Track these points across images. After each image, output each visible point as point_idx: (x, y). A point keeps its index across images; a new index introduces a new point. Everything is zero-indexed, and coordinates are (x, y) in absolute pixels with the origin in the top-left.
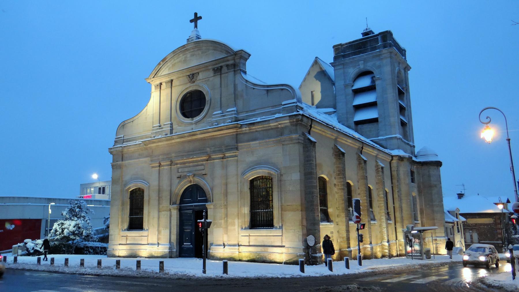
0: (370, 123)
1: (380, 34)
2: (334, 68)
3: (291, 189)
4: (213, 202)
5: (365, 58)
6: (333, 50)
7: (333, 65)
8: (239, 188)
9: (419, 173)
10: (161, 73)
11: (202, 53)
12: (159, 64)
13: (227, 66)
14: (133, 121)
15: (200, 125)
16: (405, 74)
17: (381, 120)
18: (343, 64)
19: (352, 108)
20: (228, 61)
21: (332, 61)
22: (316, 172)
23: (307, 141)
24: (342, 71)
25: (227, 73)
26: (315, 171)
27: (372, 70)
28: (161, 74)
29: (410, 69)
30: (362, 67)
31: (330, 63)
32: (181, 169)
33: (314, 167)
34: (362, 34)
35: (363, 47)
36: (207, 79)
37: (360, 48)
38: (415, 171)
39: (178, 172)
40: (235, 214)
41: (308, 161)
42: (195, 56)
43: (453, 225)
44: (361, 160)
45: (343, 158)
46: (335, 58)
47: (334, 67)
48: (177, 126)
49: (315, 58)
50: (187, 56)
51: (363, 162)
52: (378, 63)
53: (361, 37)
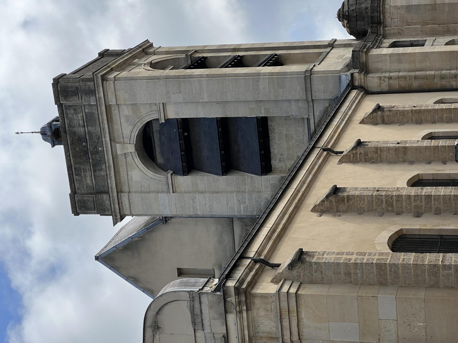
0: (268, 137)
1: (57, 101)
2: (128, 215)
3: (421, 324)
6: (82, 216)
7: (119, 217)
9: (400, 34)
16: (160, 53)
17: (263, 110)
19: (227, 176)
21: (110, 219)
22: (379, 255)
23: (295, 272)
24: (135, 198)
26: (377, 257)
27: (140, 125)
29: (149, 42)
30: (131, 148)
31: (115, 224)
33: (366, 257)
34: (53, 146)
35: (84, 144)
37: (86, 152)
38: (392, 41)
41: (348, 274)
44: (356, 153)
45: (348, 190)
46: (103, 211)
47: (125, 216)
49: (97, 261)
51: (360, 150)
52: (126, 111)
53: (60, 149)
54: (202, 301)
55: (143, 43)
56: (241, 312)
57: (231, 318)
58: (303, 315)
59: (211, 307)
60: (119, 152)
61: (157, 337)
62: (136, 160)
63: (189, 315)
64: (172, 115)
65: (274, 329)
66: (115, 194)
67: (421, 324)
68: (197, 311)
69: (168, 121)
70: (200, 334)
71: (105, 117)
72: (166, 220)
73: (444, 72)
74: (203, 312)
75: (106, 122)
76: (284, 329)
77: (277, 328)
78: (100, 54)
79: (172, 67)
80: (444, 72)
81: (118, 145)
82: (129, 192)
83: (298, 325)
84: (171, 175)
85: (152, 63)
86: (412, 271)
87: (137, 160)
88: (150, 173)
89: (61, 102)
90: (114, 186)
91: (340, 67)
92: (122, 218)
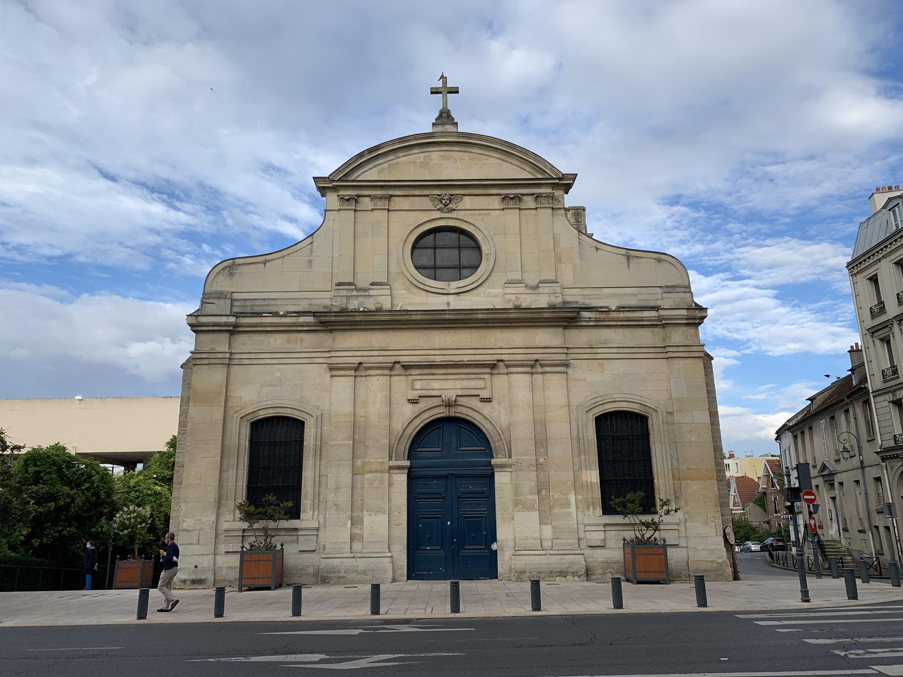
3: (693, 439)
4: (510, 457)
8: (575, 432)
10: (359, 176)
11: (471, 159)
12: (361, 155)
13: (538, 197)
14: (268, 264)
15: (468, 297)
20: (539, 185)
25: (536, 209)
28: (356, 178)
32: (419, 382)
36: (485, 212)
39: (413, 389)
40: (569, 483)
42: (452, 160)
48: (405, 292)
50: (430, 156)
54: (686, 293)
56: (687, 319)
57: (684, 312)
58: (687, 361)
59: (683, 299)
61: (653, 261)
63: (672, 284)
65: (674, 341)
67: (693, 439)
68: (678, 290)
70: (659, 290)
74: (678, 294)
76: (677, 348)
77: (675, 342)
83: (680, 357)
86: (716, 435)
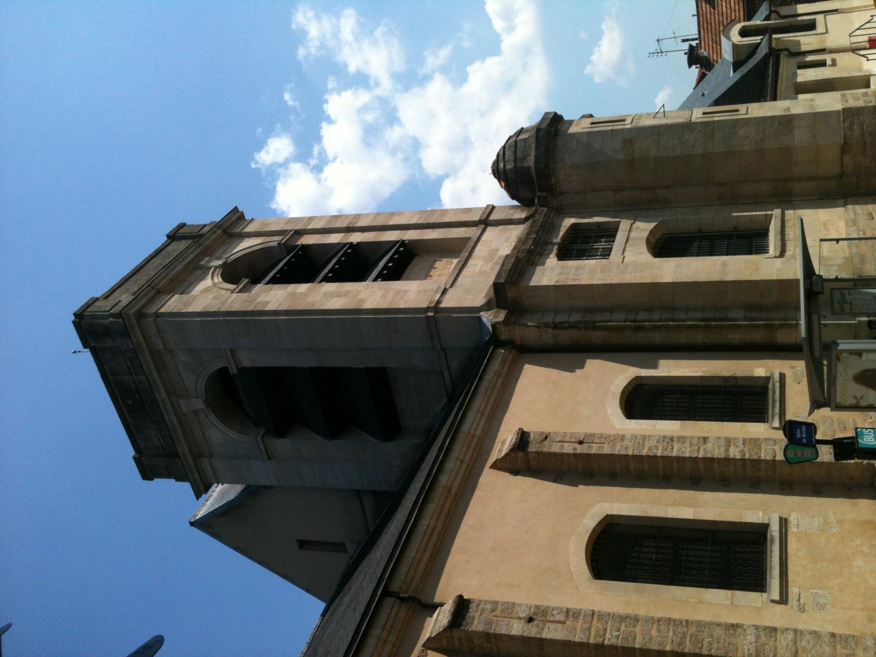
5: (168, 394)
7: (202, 488)
18: (197, 456)
35: (137, 396)
43: (786, 53)
55: (227, 217)
60: (185, 410)
62: (210, 417)
64: (247, 360)
66: (191, 461)
69: (244, 370)
71: (152, 367)
72: (266, 488)
73: (641, 316)
75: (155, 373)
78: (168, 236)
79: (247, 280)
80: (641, 316)
81: (181, 402)
82: (211, 456)
84: (262, 437)
85: (228, 262)
87: (212, 418)
88: (233, 434)
89: (93, 345)
90: (187, 452)
91: (479, 300)
92: (207, 488)
